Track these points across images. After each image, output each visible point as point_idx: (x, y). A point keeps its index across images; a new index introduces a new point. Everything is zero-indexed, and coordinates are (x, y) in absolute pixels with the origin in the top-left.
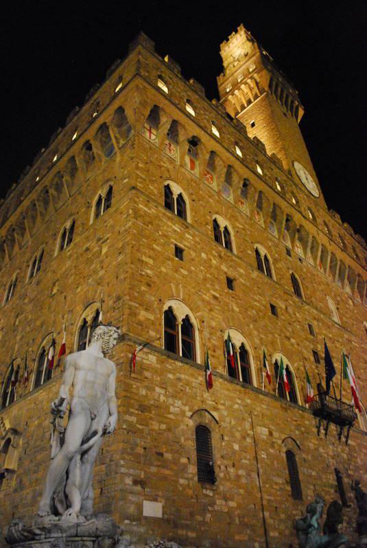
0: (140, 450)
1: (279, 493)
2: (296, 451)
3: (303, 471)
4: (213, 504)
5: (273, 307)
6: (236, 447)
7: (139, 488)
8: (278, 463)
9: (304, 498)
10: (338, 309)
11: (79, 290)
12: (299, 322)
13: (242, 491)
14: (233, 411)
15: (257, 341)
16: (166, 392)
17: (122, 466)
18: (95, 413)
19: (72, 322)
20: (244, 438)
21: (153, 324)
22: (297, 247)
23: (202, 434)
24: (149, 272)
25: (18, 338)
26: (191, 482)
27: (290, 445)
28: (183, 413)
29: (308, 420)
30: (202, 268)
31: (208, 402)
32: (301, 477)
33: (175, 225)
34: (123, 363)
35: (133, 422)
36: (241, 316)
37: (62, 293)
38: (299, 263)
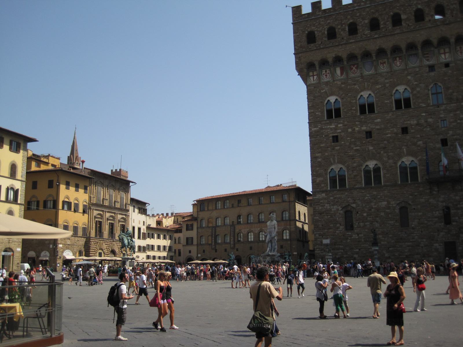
0: (321, 226)
1: (390, 227)
4: (351, 236)
6: (365, 214)
7: (321, 237)
12: (429, 125)
20: (370, 210)
22: (445, 53)
23: (348, 214)
24: (319, 160)
26: (341, 232)
28: (338, 210)
30: (348, 138)
31: (350, 201)
33: (331, 125)
36: (374, 150)
38: (444, 69)
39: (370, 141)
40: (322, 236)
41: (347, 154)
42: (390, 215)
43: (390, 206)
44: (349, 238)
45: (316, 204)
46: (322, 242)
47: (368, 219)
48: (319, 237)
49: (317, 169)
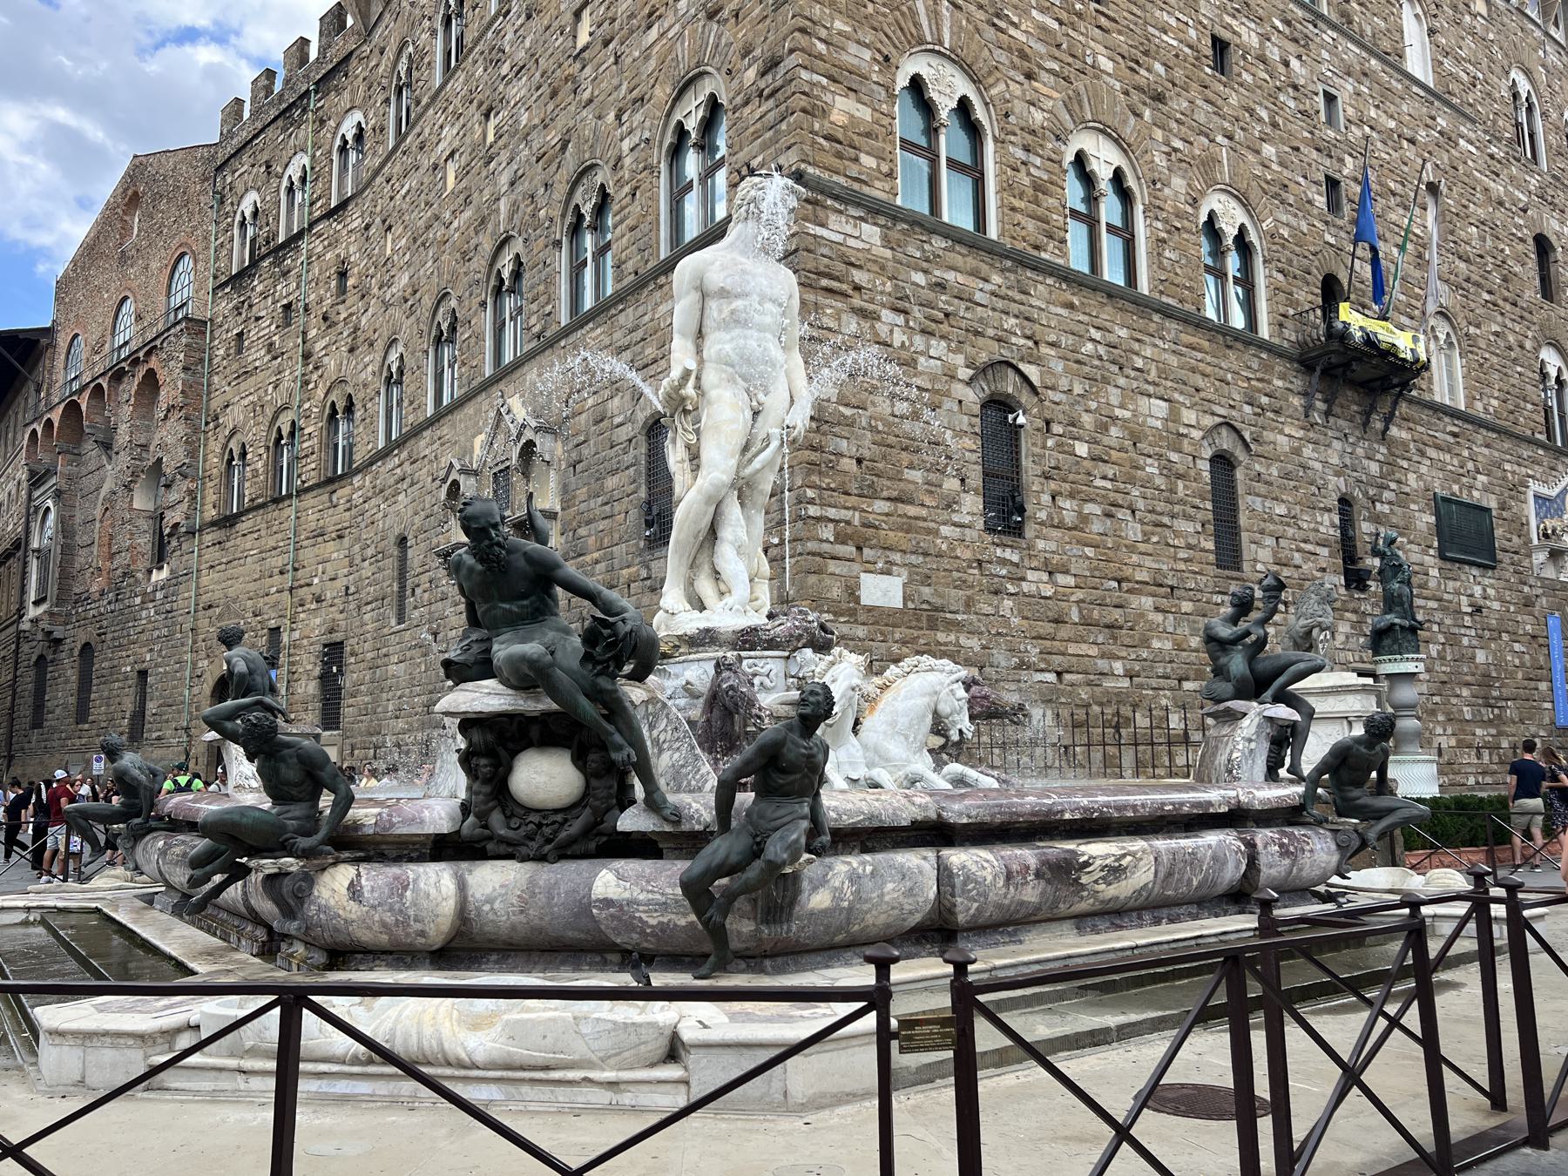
0: (848, 464)
2: (1240, 454)
3: (1249, 505)
5: (1220, 47)
6: (1082, 449)
7: (850, 550)
8: (1185, 487)
9: (1246, 566)
10: (1432, 32)
11: (654, 33)
12: (1295, 88)
13: (1089, 552)
14: (1078, 362)
15: (1160, 160)
16: (907, 322)
17: (811, 502)
18: (761, 396)
19: (647, 135)
20: (1103, 428)
21: (868, 135)
25: (504, 179)
26: (970, 534)
27: (1226, 441)
29: (1282, 377)
31: (1014, 340)
32: (1243, 520)
34: (796, 251)
35: (828, 400)
36: (1118, 86)
37: (606, 43)
39: (1103, 21)
40: (859, 548)
41: (1002, 24)
42: (1180, 484)
43: (1183, 430)
44: (1011, 589)
45: (825, 282)
46: (852, 592)
47: (1099, 483)
48: (841, 550)
49: (839, 25)
